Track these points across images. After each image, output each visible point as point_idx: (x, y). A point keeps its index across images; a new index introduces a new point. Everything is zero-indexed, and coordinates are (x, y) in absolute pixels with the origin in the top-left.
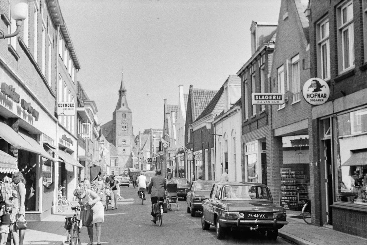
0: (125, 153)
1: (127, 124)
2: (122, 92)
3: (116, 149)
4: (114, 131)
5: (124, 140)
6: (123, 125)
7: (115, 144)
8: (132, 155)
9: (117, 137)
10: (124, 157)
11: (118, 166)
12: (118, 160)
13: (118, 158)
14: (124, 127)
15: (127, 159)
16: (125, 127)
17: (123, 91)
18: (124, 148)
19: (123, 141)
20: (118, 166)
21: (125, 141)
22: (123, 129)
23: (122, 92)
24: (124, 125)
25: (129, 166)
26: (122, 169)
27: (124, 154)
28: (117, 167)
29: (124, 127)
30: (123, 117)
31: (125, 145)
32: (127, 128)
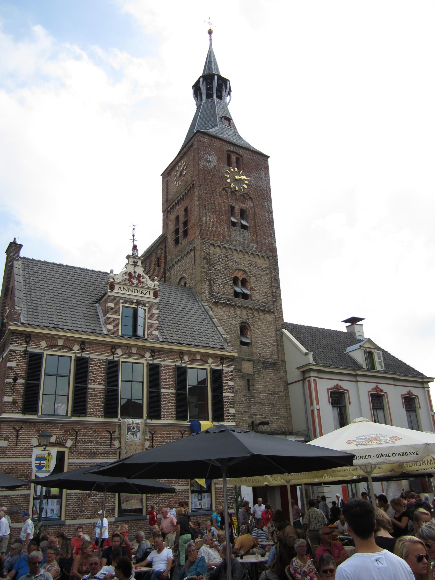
5: (241, 276)
16: (243, 213)
21: (244, 283)
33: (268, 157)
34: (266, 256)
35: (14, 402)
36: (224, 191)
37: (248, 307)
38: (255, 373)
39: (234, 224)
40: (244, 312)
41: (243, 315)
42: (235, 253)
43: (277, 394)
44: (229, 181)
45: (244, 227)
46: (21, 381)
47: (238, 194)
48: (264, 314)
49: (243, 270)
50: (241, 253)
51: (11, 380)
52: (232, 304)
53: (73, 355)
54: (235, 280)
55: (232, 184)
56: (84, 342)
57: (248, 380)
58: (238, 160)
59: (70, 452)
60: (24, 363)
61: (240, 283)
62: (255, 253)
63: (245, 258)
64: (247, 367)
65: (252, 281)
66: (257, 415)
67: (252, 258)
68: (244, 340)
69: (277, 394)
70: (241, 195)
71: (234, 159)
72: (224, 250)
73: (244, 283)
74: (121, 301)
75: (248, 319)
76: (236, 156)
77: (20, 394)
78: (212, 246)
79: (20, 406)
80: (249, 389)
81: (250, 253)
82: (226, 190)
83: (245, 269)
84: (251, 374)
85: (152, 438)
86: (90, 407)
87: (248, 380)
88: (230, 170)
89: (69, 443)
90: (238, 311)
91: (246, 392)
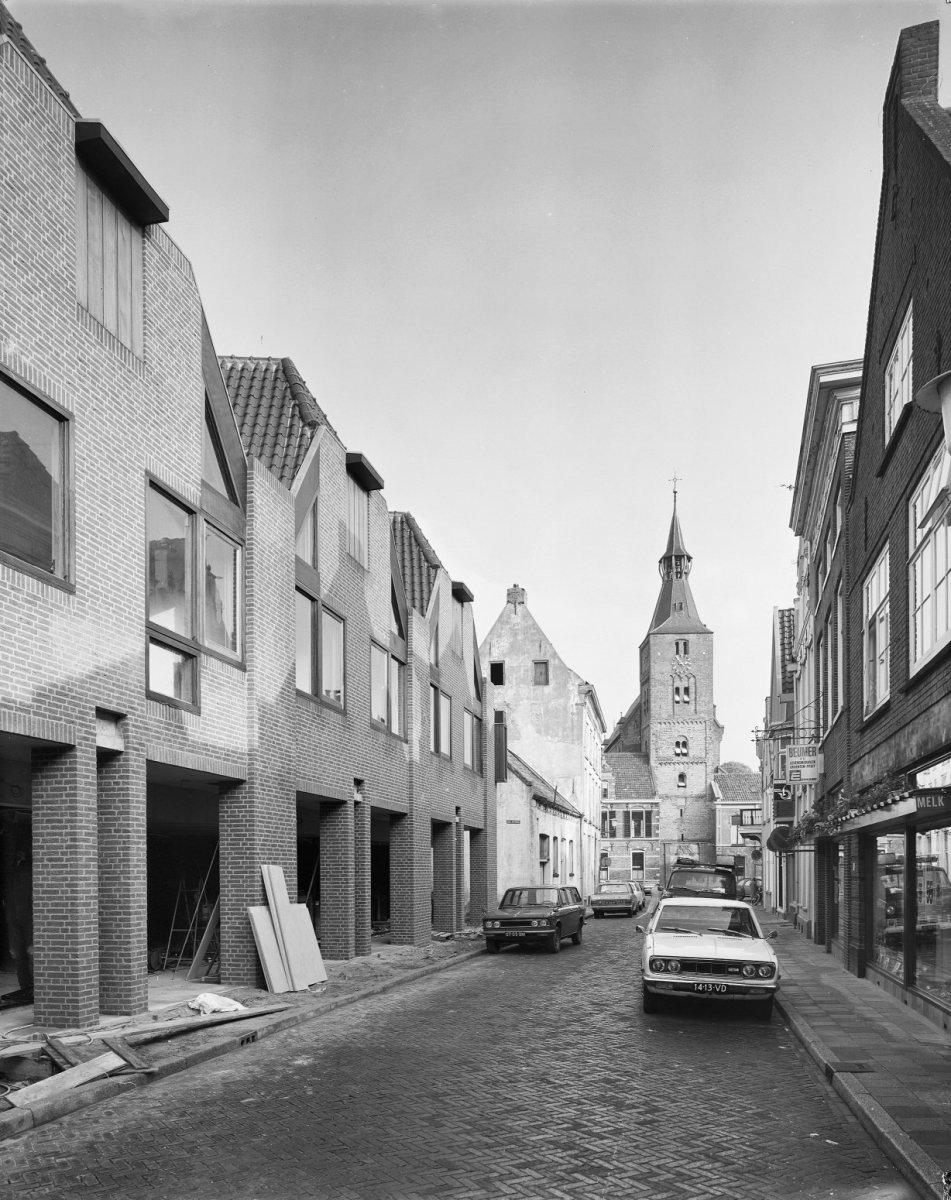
0: (685, 787)
1: (692, 680)
3: (650, 773)
4: (643, 708)
5: (681, 740)
6: (677, 684)
7: (646, 758)
8: (712, 794)
9: (655, 727)
12: (658, 813)
13: (656, 804)
14: (682, 691)
15: (695, 809)
16: (687, 690)
17: (679, 557)
18: (681, 768)
20: (657, 835)
21: (685, 744)
22: (677, 698)
23: (674, 561)
24: (682, 685)
25: (698, 837)
26: (674, 848)
27: (682, 789)
29: (682, 691)
30: (677, 653)
31: (685, 759)
32: (692, 696)
39: (678, 702)
45: (687, 702)
54: (678, 744)
58: (685, 644)
64: (682, 802)
67: (691, 725)
73: (685, 744)
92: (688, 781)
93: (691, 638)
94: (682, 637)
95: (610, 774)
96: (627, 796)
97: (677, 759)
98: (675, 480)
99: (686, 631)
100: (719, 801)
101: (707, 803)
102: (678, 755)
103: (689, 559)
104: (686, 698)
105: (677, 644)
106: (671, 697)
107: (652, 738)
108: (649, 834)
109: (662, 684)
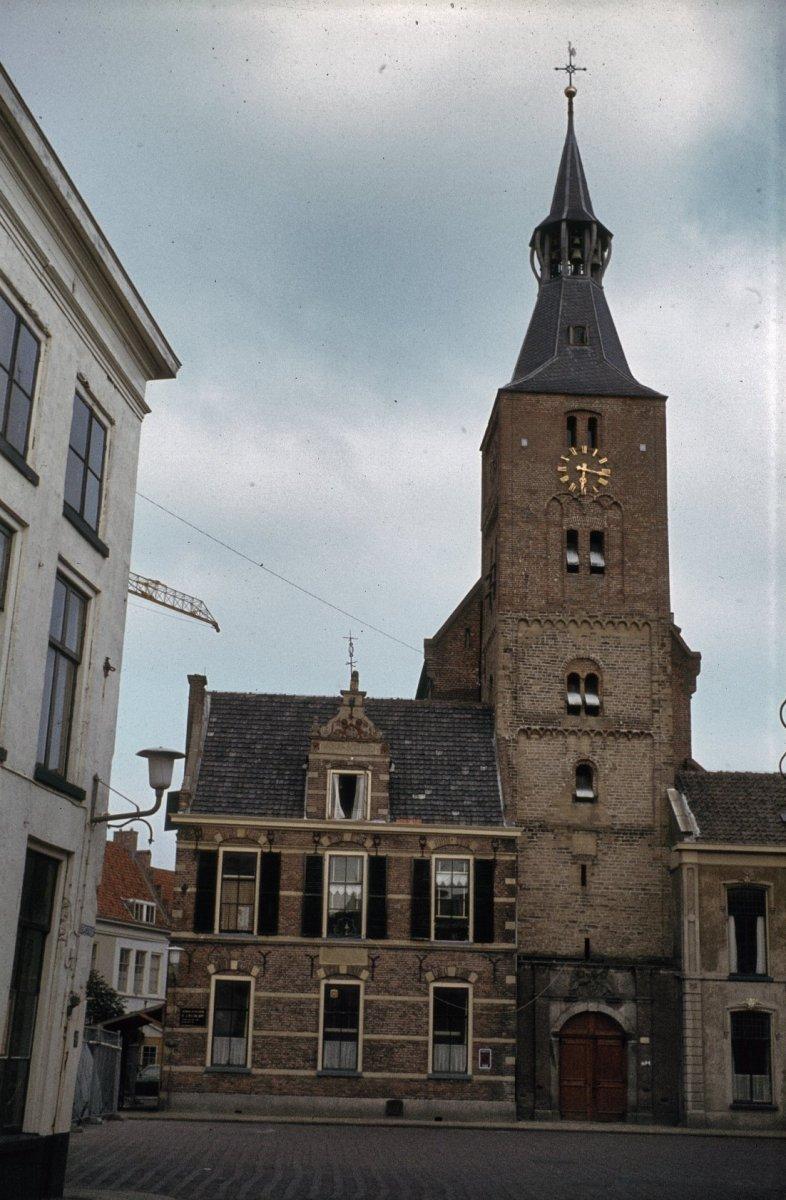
2: (564, 226)
5: (583, 672)
6: (575, 521)
10: (584, 843)
11: (509, 936)
12: (513, 870)
13: (510, 843)
14: (584, 541)
19: (573, 682)
20: (509, 936)
21: (592, 684)
26: (561, 978)
28: (498, 946)
29: (584, 541)
31: (592, 722)
33: (664, 398)
34: (643, 621)
35: (185, 918)
36: (556, 504)
37: (592, 731)
38: (600, 854)
39: (573, 569)
40: (585, 742)
41: (585, 745)
42: (572, 627)
43: (644, 890)
44: (565, 479)
46: (192, 890)
47: (586, 502)
48: (629, 740)
49: (589, 659)
50: (585, 626)
51: (179, 890)
52: (559, 728)
53: (258, 851)
55: (573, 484)
56: (272, 831)
57: (584, 868)
58: (592, 425)
59: (257, 983)
60: (194, 867)
61: (582, 685)
62: (616, 621)
63: (594, 634)
64: (584, 843)
65: (606, 678)
66: (597, 927)
67: (610, 630)
68: (581, 794)
69: (644, 890)
70: (594, 502)
71: (582, 426)
72: (547, 626)
74: (329, 766)
75: (594, 752)
76: (588, 416)
77: (190, 906)
78: (522, 624)
79: (190, 924)
80: (584, 882)
81: (604, 624)
82: (559, 501)
83: (593, 656)
84: (590, 855)
85: (374, 966)
86: (282, 921)
87: (584, 868)
88: (569, 455)
89: (256, 971)
90: (572, 740)
91: (577, 888)
92: (598, 784)
93: (609, 408)
94: (585, 404)
95: (376, 749)
96: (428, 814)
97: (571, 721)
98: (571, 69)
99: (591, 390)
100: (687, 844)
101: (658, 851)
102: (573, 710)
103: (605, 236)
104: (596, 560)
105: (571, 424)
106: (555, 555)
107: (505, 659)
108: (485, 933)
109: (531, 519)
